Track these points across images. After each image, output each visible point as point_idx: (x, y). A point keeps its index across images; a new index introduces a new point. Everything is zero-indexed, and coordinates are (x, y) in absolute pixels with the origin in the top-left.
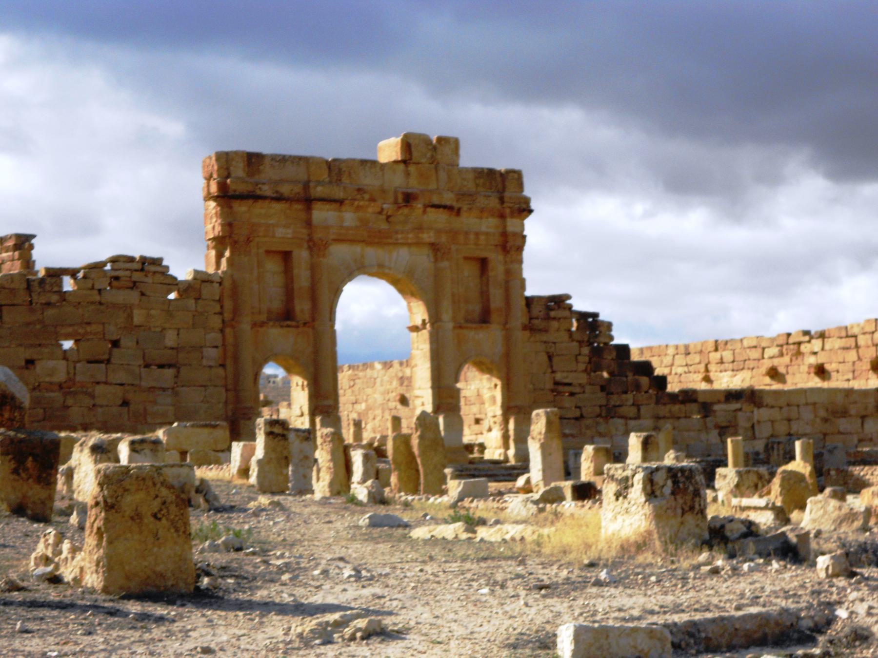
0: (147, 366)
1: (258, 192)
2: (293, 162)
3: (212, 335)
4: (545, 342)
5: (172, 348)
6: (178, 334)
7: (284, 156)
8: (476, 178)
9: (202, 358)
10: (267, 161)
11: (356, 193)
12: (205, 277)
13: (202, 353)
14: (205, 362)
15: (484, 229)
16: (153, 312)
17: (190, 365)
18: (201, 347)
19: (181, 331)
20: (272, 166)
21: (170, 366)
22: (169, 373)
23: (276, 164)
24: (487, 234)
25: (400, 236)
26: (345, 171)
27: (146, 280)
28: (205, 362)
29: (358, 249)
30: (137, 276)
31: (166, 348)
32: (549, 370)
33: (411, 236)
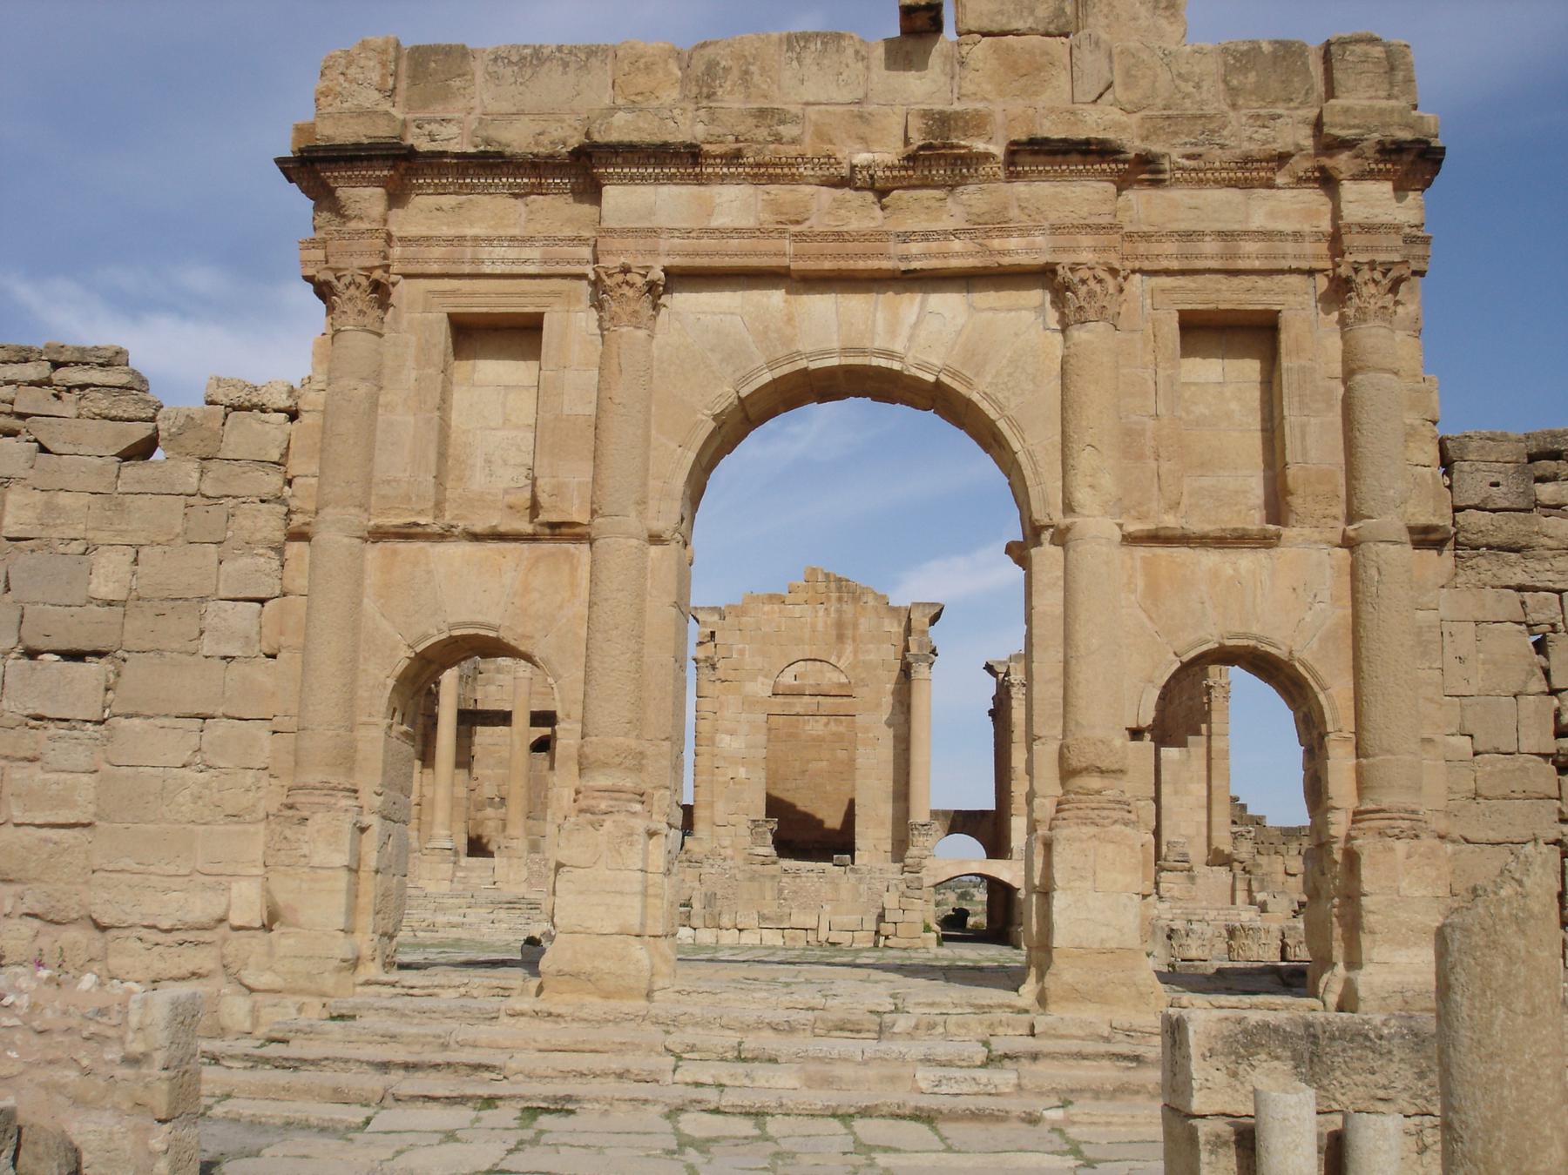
0: (32, 654)
1: (423, 145)
2: (566, 65)
3: (245, 562)
4: (1520, 588)
5: (110, 603)
6: (136, 562)
7: (537, 52)
8: (1229, 70)
9: (202, 633)
10: (478, 67)
11: (751, 121)
12: (235, 396)
13: (202, 617)
14: (208, 646)
15: (1258, 221)
16: (64, 499)
17: (159, 651)
18: (203, 599)
19: (144, 551)
20: (494, 77)
21: (100, 654)
22: (93, 669)
23: (509, 71)
24: (1266, 235)
25: (915, 248)
26: (727, 70)
27: (56, 408)
28: (208, 646)
29: (774, 299)
30: (28, 400)
31: (92, 600)
32: (1538, 684)
33: (956, 245)
